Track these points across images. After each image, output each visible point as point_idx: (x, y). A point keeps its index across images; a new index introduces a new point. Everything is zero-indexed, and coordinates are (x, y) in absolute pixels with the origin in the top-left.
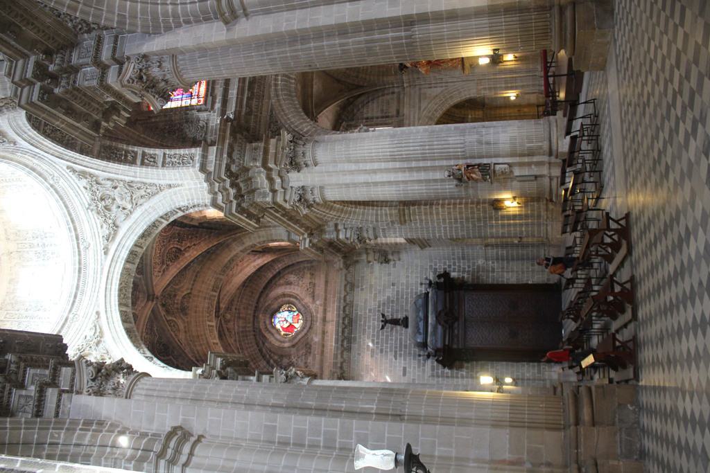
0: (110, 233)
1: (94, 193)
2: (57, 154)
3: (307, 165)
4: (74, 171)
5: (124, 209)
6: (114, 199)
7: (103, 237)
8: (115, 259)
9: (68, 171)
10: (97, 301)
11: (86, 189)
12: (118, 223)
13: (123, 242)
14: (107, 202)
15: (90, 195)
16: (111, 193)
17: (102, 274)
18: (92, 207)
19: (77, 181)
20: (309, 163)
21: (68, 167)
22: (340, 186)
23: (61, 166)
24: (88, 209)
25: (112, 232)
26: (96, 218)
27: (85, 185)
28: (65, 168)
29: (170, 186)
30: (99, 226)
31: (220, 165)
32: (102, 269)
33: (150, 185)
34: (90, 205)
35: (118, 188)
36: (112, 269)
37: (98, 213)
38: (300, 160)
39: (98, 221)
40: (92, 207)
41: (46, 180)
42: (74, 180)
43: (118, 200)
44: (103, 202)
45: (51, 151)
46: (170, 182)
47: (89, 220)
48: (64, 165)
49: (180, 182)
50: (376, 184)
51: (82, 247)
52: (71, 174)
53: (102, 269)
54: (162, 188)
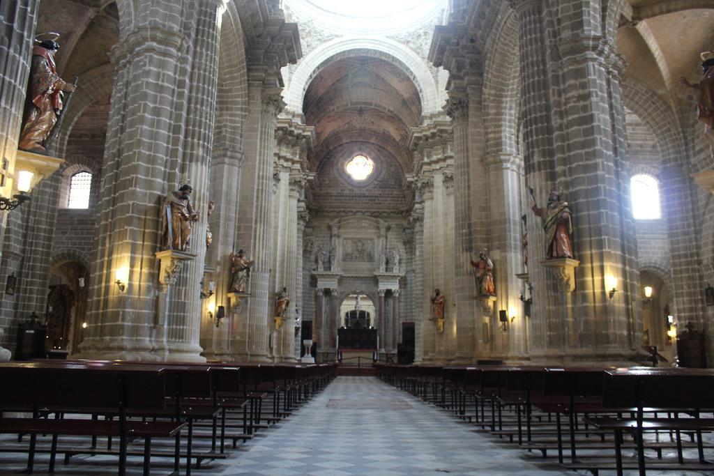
1: (315, 32)
3: (292, 190)
4: (337, 36)
20: (293, 192)
21: (342, 36)
22: (277, 206)
30: (300, 17)
31: (283, 123)
37: (305, 24)
38: (296, 188)
44: (307, 31)
45: (361, 41)
46: (292, 82)
49: (290, 90)
50: (276, 233)
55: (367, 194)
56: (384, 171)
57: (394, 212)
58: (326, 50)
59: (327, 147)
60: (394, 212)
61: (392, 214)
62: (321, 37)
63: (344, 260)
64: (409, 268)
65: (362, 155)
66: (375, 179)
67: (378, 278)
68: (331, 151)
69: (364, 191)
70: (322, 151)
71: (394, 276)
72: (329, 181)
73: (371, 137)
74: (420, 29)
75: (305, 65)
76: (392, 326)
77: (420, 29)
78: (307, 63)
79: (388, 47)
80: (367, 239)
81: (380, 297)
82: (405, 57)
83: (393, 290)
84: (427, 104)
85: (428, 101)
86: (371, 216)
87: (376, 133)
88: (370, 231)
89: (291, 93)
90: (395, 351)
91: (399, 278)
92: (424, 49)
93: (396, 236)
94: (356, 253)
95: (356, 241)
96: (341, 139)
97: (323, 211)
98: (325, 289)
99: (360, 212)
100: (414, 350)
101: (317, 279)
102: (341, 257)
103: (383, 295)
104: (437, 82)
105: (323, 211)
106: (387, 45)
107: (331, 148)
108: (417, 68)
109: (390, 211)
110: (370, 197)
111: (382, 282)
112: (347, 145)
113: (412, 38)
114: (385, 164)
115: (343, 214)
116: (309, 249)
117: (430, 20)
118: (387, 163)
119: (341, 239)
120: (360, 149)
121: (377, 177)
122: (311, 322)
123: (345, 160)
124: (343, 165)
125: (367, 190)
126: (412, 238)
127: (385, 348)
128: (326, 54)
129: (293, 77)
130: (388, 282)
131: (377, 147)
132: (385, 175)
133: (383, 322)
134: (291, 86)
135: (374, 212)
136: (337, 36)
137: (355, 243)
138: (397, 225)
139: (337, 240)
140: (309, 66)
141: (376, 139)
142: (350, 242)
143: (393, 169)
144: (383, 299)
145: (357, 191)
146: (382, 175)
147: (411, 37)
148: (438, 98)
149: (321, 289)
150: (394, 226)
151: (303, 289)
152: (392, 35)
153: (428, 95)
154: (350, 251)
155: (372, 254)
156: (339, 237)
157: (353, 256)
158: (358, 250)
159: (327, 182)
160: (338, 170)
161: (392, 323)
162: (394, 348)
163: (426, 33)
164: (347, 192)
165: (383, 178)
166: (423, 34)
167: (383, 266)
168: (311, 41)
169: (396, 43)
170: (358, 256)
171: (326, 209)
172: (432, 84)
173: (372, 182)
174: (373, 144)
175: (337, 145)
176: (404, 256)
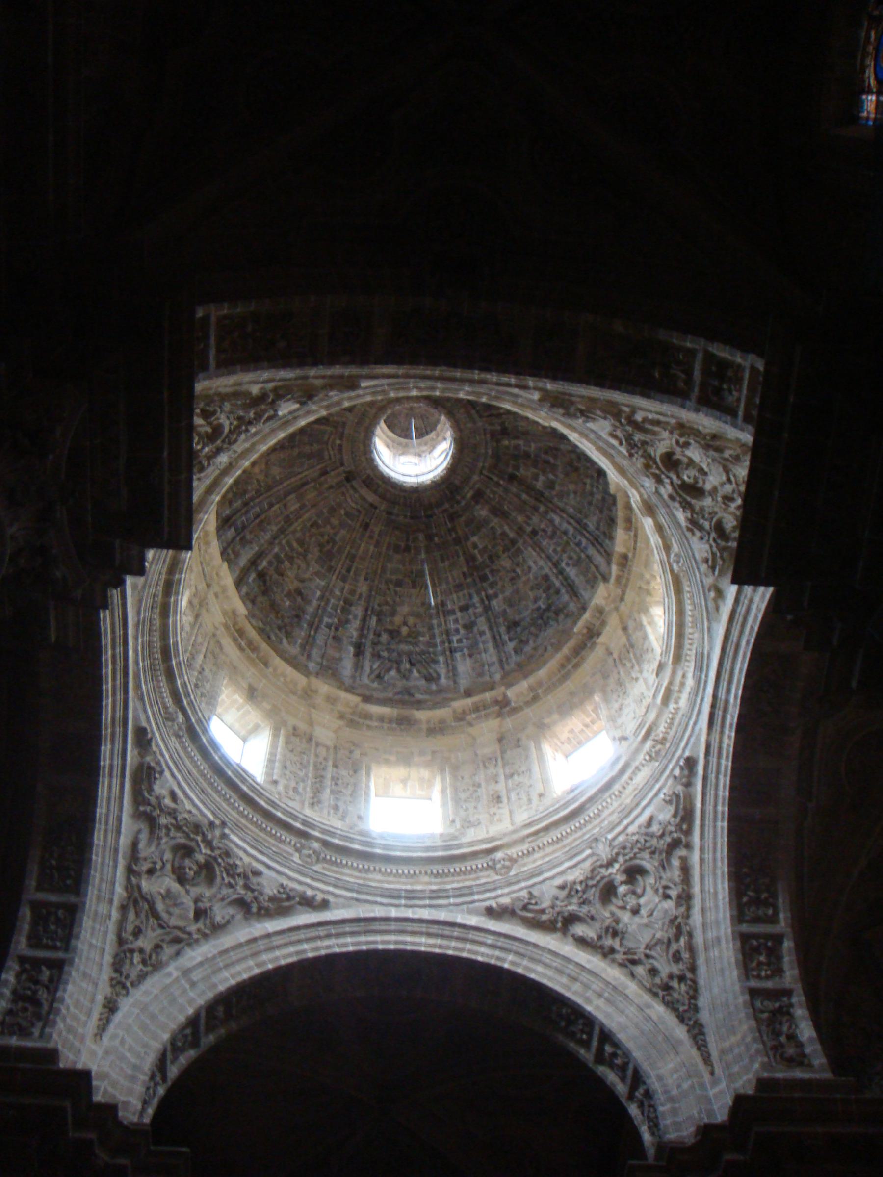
0: (150, 790)
1: (231, 870)
2: (376, 926)
4: (309, 903)
5: (151, 872)
6: (182, 880)
7: (161, 773)
8: (119, 730)
9: (320, 897)
10: (140, 601)
11: (257, 873)
12: (144, 827)
13: (116, 782)
14: (195, 868)
15: (238, 862)
16: (195, 891)
17: (137, 676)
18: (217, 833)
19: (285, 882)
21: (324, 905)
23: (341, 900)
24: (224, 824)
25: (146, 794)
26: (194, 811)
27: (259, 880)
28: (331, 899)
29: (111, 1007)
32: (138, 686)
33: (142, 977)
34: (224, 836)
35: (191, 914)
36: (119, 697)
37: (197, 828)
39: (188, 806)
40: (217, 833)
41: (325, 844)
42: (290, 878)
43: (176, 887)
44: (201, 859)
45: (393, 926)
46: (118, 1017)
47: (203, 796)
48: (338, 907)
51: (180, 718)
52: (309, 893)
53: (138, 686)
54: (119, 988)
58: (261, 945)
62: (249, 896)
74: (610, 864)
75: (175, 974)
77: (610, 864)
78: (186, 972)
79: (493, 947)
82: (560, 972)
84: (674, 1112)
85: (672, 1099)
89: (107, 1053)
92: (632, 928)
104: (697, 1032)
106: (490, 940)
108: (608, 1001)
113: (584, 903)
117: (643, 819)
128: (264, 957)
129: (126, 1005)
134: (111, 1028)
136: (309, 903)
140: (193, 984)
147: (575, 900)
148: (715, 1083)
152: (506, 901)
153: (670, 1081)
163: (634, 873)
166: (620, 878)
168: (210, 900)
169: (521, 932)
172: (680, 1042)
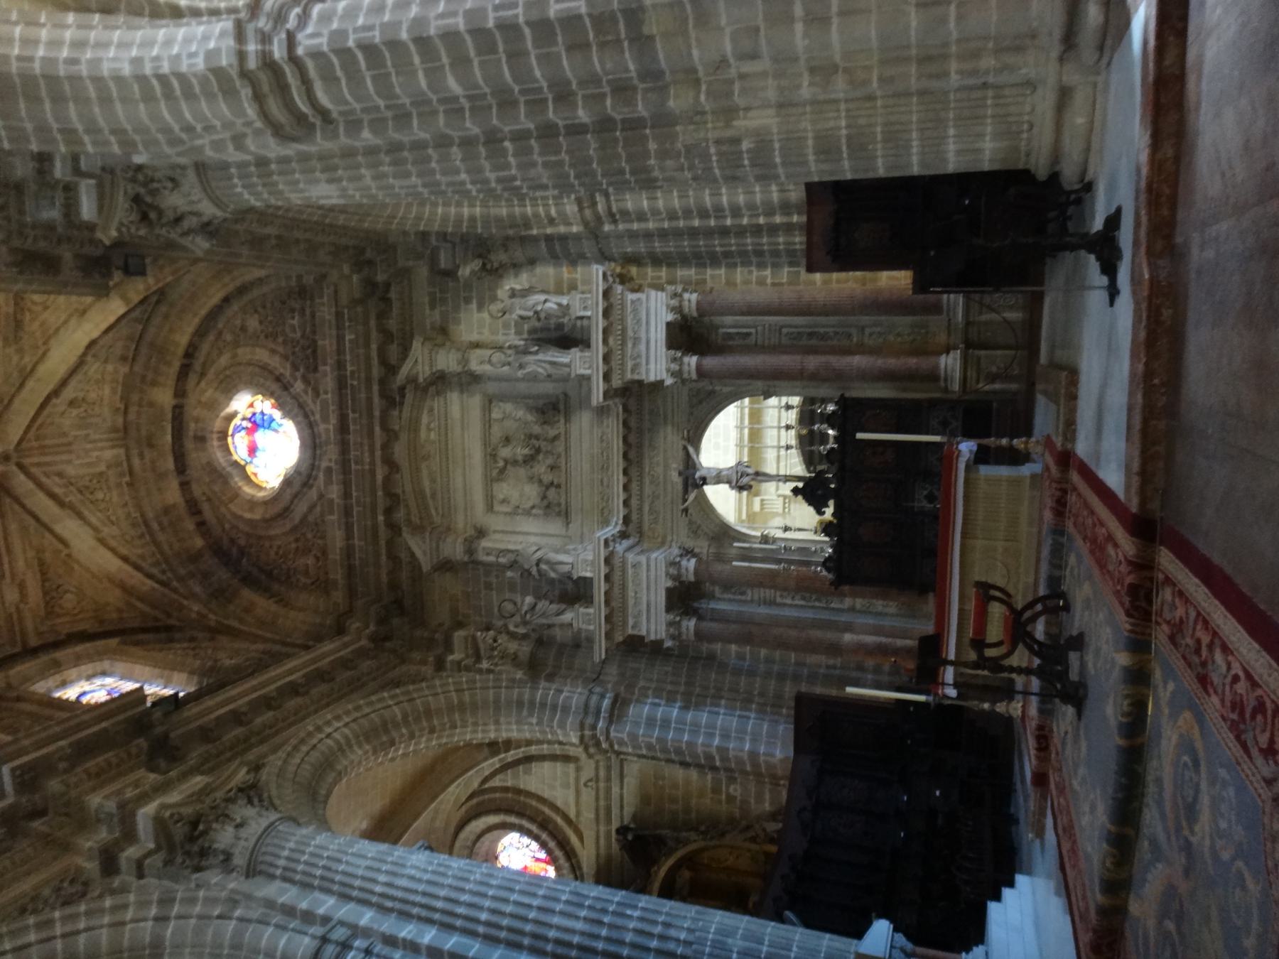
55: (333, 420)
56: (262, 355)
57: (382, 316)
59: (194, 558)
60: (382, 316)
61: (393, 324)
63: (565, 514)
64: (588, 247)
65: (223, 435)
66: (286, 388)
67: (616, 382)
68: (217, 549)
69: (328, 428)
70: (206, 576)
71: (606, 313)
72: (307, 551)
73: (151, 404)
76: (833, 320)
80: (487, 423)
81: (701, 373)
83: (670, 317)
86: (402, 404)
87: (132, 390)
88: (455, 410)
90: (955, 302)
91: (619, 288)
93: (474, 306)
94: (541, 468)
95: (497, 470)
96: (167, 510)
97: (394, 586)
98: (669, 609)
99: (386, 447)
100: (965, 182)
101: (632, 637)
102: (555, 527)
103: (693, 360)
105: (394, 586)
107: (199, 542)
109: (374, 334)
110: (341, 406)
111: (635, 368)
112: (194, 486)
114: (240, 351)
115: (400, 515)
116: (525, 649)
118: (236, 344)
119: (494, 522)
120: (201, 439)
121: (278, 379)
122: (800, 699)
123: (236, 495)
124: (252, 504)
125: (325, 419)
126: (464, 239)
127: (939, 354)
130: (636, 340)
131: (192, 379)
132: (273, 351)
133: (812, 362)
135: (383, 395)
137: (502, 471)
138: (433, 307)
139: (485, 543)
141: (154, 383)
142: (504, 490)
143: (253, 323)
144: (711, 362)
145: (331, 456)
146: (275, 362)
149: (670, 624)
150: (437, 312)
151: (670, 700)
154: (532, 492)
155: (541, 402)
156: (481, 533)
157: (547, 478)
158: (529, 460)
159: (310, 561)
160: (268, 522)
161: (822, 320)
162: (936, 309)
164: (335, 492)
165: (286, 357)
167: (577, 362)
170: (549, 461)
171: (384, 578)
173: (295, 397)
174: (180, 393)
175: (190, 525)
176: (547, 272)
